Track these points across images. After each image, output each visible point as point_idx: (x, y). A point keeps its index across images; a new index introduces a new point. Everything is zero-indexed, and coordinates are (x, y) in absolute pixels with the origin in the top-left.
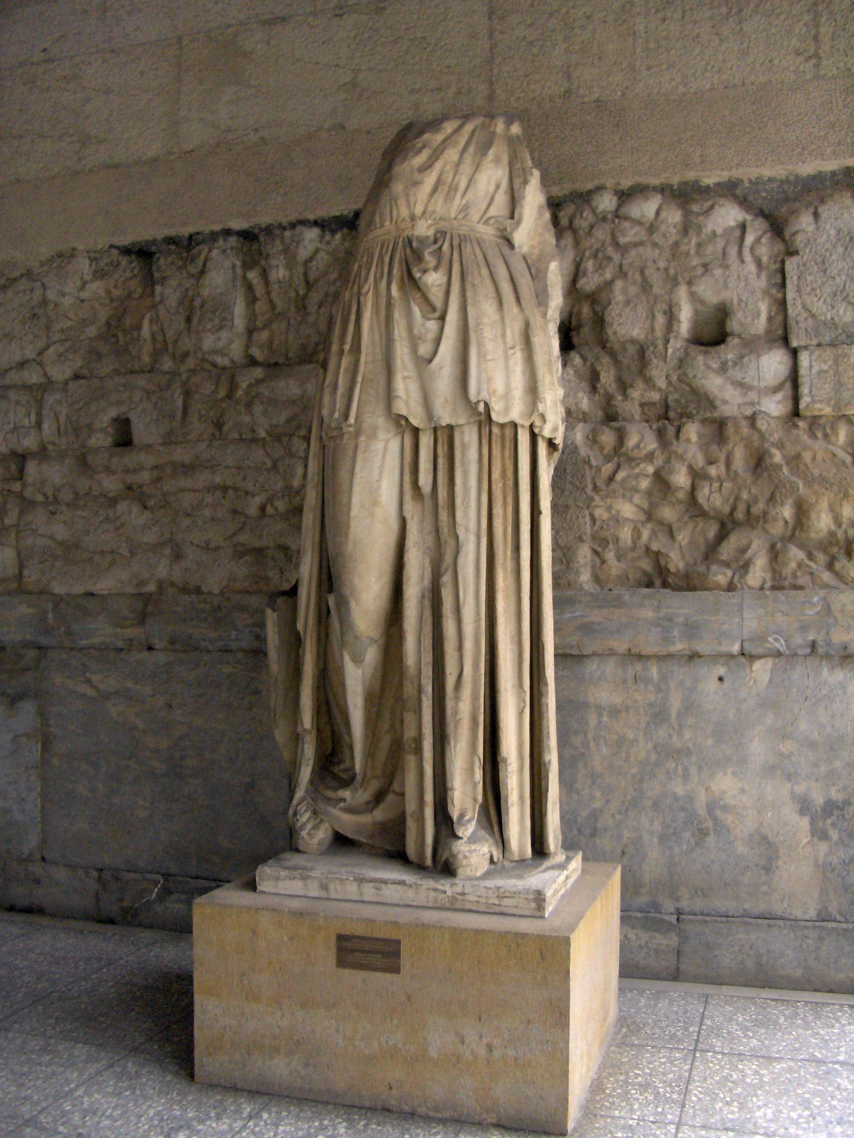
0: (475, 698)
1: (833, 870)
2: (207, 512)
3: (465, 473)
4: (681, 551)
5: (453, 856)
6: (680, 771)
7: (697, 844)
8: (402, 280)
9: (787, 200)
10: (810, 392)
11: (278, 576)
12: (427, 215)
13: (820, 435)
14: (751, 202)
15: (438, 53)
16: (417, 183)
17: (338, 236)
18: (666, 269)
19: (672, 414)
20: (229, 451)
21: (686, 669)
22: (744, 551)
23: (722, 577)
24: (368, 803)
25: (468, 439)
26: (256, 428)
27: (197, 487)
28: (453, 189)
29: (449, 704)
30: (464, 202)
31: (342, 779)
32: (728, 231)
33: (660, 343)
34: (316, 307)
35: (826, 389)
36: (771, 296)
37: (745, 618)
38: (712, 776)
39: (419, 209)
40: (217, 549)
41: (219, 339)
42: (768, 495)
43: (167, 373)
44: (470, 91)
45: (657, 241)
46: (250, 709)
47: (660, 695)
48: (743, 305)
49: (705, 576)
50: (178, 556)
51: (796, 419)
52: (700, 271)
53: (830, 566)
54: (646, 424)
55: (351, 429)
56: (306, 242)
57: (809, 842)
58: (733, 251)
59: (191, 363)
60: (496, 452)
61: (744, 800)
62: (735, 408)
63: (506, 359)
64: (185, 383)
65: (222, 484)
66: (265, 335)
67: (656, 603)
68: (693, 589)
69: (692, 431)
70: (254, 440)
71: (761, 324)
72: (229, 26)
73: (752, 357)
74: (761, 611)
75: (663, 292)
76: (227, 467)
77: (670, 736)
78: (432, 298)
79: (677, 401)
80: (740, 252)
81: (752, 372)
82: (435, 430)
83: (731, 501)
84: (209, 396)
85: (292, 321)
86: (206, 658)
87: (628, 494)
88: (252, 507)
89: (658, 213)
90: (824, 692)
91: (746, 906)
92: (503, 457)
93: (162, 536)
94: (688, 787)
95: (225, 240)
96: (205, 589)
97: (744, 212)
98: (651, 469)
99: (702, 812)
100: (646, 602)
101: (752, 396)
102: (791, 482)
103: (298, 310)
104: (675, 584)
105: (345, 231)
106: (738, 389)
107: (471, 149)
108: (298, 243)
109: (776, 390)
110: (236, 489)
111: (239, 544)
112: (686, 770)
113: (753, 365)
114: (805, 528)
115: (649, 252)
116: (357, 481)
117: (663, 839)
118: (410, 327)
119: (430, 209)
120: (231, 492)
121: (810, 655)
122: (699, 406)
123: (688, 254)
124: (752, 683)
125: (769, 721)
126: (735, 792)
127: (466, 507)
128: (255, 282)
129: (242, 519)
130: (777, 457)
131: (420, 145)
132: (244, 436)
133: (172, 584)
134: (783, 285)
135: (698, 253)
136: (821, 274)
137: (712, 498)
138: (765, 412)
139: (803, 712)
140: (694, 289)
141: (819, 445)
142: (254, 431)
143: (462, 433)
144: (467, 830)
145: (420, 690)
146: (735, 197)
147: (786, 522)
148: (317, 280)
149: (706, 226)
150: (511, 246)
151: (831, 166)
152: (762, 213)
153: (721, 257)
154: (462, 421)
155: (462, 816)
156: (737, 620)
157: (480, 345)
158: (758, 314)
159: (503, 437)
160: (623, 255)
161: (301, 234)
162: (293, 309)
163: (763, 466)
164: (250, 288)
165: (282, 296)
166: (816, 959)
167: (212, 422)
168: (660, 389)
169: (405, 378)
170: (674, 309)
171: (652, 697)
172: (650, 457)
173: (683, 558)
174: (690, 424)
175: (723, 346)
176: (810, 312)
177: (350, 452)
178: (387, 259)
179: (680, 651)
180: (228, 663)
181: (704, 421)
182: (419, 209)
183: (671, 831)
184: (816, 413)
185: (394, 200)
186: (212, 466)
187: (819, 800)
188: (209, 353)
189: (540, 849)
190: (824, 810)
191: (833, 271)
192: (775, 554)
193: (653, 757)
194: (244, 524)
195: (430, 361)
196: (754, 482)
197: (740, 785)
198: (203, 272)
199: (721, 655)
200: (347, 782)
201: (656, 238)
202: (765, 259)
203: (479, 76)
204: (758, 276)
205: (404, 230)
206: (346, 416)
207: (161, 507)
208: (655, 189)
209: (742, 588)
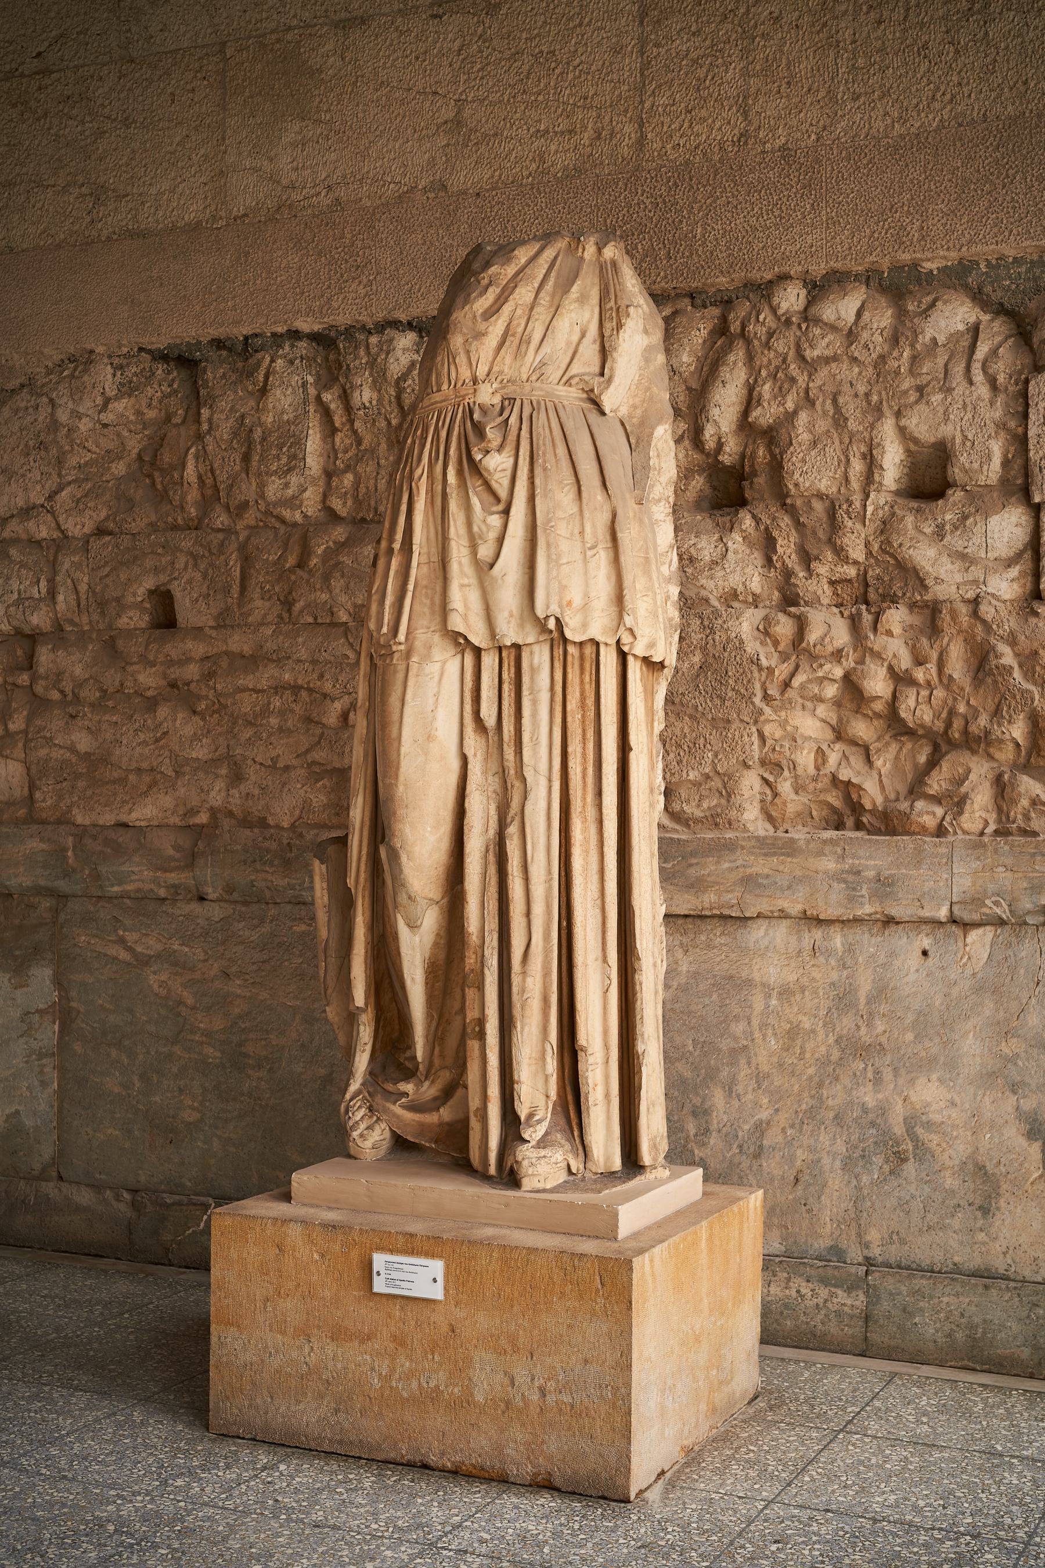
0: (546, 974)
2: (274, 721)
3: (535, 702)
4: (881, 781)
6: (870, 1075)
8: (460, 462)
12: (492, 377)
14: (988, 295)
15: (570, 76)
16: (479, 335)
18: (867, 395)
19: (872, 596)
20: (300, 640)
21: (879, 939)
22: (961, 782)
25: (539, 659)
28: (524, 341)
29: (516, 980)
30: (538, 359)
32: (954, 337)
33: (857, 499)
36: (1008, 431)
39: (482, 371)
40: (287, 768)
41: (287, 485)
42: (991, 705)
43: (219, 530)
44: (612, 134)
45: (856, 354)
47: (845, 973)
48: (968, 444)
50: (237, 777)
52: (913, 396)
54: (836, 610)
55: (402, 647)
56: (399, 353)
59: (251, 517)
62: (954, 588)
63: (585, 562)
64: (242, 547)
66: (348, 479)
67: (839, 850)
68: (892, 832)
69: (896, 618)
70: (333, 625)
71: (994, 470)
72: (290, 29)
73: (978, 518)
74: (976, 865)
75: (861, 428)
76: (299, 661)
77: (858, 1027)
78: (495, 485)
79: (878, 578)
80: (968, 369)
81: (977, 540)
83: (944, 715)
84: (275, 564)
85: (383, 462)
86: (273, 911)
87: (809, 704)
89: (859, 314)
92: (582, 682)
93: (216, 750)
94: (880, 1096)
95: (292, 346)
96: (271, 821)
97: (977, 310)
98: (838, 672)
100: (827, 849)
103: (390, 445)
107: (549, 286)
108: (388, 353)
109: (1010, 562)
110: (310, 690)
112: (877, 1072)
113: (979, 529)
115: (845, 371)
116: (408, 711)
117: (848, 1165)
118: (469, 524)
119: (496, 369)
120: (304, 694)
122: (906, 585)
123: (897, 373)
124: (965, 960)
125: (988, 1013)
127: (536, 743)
128: (333, 406)
129: (318, 731)
130: (1007, 657)
131: (486, 281)
132: (319, 621)
133: (230, 814)
134: (1026, 416)
135: (911, 371)
138: (993, 595)
140: (903, 422)
143: (531, 653)
144: (533, 1134)
146: (966, 287)
147: (1018, 745)
152: (1001, 310)
153: (942, 376)
154: (530, 639)
158: (989, 458)
159: (582, 658)
160: (810, 375)
161: (391, 340)
162: (384, 446)
164: (326, 413)
168: (856, 563)
169: (462, 586)
171: (834, 976)
172: (838, 655)
173: (882, 788)
174: (892, 611)
177: (400, 676)
178: (443, 434)
179: (870, 915)
181: (912, 606)
182: (482, 371)
185: (452, 357)
186: (280, 660)
188: (275, 504)
192: (1002, 789)
193: (836, 1054)
198: (264, 391)
201: (856, 350)
202: (1001, 379)
203: (626, 111)
204: (992, 403)
207: (214, 712)
208: (857, 277)
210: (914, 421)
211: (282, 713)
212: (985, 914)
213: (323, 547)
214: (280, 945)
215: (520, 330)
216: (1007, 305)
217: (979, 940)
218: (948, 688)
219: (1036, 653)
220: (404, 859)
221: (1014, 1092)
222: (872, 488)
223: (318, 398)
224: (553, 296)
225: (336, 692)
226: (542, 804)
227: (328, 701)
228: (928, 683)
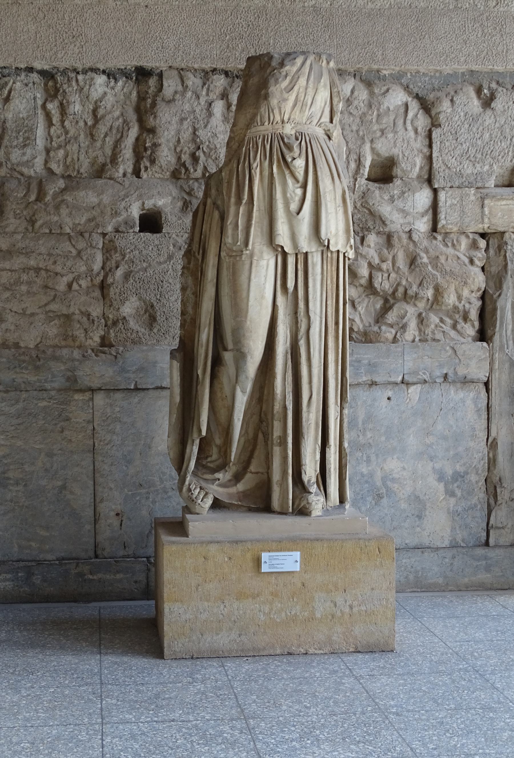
0: (317, 412)
1: (458, 515)
2: (24, 288)
3: (314, 280)
5: (308, 503)
6: (365, 459)
7: (376, 504)
9: (434, 90)
10: (445, 218)
11: (83, 335)
12: (291, 120)
13: (450, 244)
14: (412, 89)
16: (285, 100)
17: (120, 83)
18: (357, 131)
20: (41, 242)
21: (368, 393)
22: (403, 317)
23: (389, 333)
24: (230, 481)
25: (315, 259)
26: (63, 226)
27: (13, 268)
29: (304, 415)
31: (210, 467)
32: (397, 107)
34: (102, 136)
35: (454, 217)
37: (406, 360)
38: (385, 460)
40: (33, 315)
41: (24, 154)
42: (418, 282)
45: (352, 111)
46: (62, 432)
47: (352, 410)
49: (378, 334)
51: (434, 234)
52: (379, 134)
53: (454, 327)
56: (97, 86)
57: (444, 499)
58: (400, 122)
60: (329, 267)
61: (405, 474)
62: (399, 226)
63: (336, 213)
65: (35, 266)
66: (61, 153)
70: (61, 234)
73: (410, 193)
77: (358, 436)
78: (297, 174)
80: (405, 123)
81: (410, 203)
82: (297, 255)
84: (22, 198)
86: (24, 395)
88: (61, 285)
89: (352, 92)
90: (451, 405)
91: (407, 542)
95: (27, 76)
96: (22, 344)
99: (379, 483)
101: (410, 219)
102: (433, 275)
104: (357, 339)
105: (124, 79)
106: (401, 214)
108: (90, 86)
110: (47, 271)
111: (50, 311)
114: (440, 303)
116: (252, 284)
119: (292, 117)
120: (43, 272)
121: (443, 382)
122: (375, 223)
123: (371, 122)
126: (399, 469)
127: (315, 300)
128: (53, 112)
129: (53, 293)
131: (284, 73)
132: (53, 231)
134: (430, 146)
135: (377, 121)
136: (455, 141)
137: (383, 283)
138: (417, 230)
139: (439, 417)
140: (374, 146)
141: (450, 251)
142: (61, 228)
143: (313, 256)
145: (285, 408)
146: (401, 84)
147: (428, 300)
148: (103, 117)
149: (383, 103)
150: (330, 138)
151: (462, 68)
152: (417, 97)
153: (392, 125)
154: (313, 250)
155: (309, 481)
156: (401, 362)
157: (326, 205)
158: (415, 165)
159: (332, 258)
161: (92, 79)
162: (82, 136)
163: (416, 264)
164: (48, 116)
165: (73, 124)
166: (451, 570)
167: (26, 219)
170: (361, 159)
173: (362, 321)
174: (370, 235)
175: (391, 184)
176: (447, 166)
178: (268, 147)
179: (364, 382)
180: (43, 399)
181: (378, 233)
183: (360, 496)
184: (448, 231)
185: (270, 110)
187: (449, 472)
189: (342, 500)
190: (452, 478)
191: (461, 139)
192: (421, 320)
194: (55, 296)
195: (298, 214)
196: (411, 273)
197: (402, 465)
199: (390, 383)
200: (222, 467)
201: (352, 109)
202: (419, 129)
205: (277, 129)
206: (246, 244)
209: (402, 341)
210: (380, 145)
211: (29, 283)
212: (419, 379)
213: (53, 190)
214: (30, 414)
215: (302, 99)
216: (420, 95)
217: (414, 391)
218: (397, 273)
219: (438, 257)
220: (249, 358)
221: (432, 461)
222: (358, 176)
223: (44, 106)
224: (314, 83)
225: (64, 272)
226: (318, 329)
227: (59, 277)
228: (388, 270)
